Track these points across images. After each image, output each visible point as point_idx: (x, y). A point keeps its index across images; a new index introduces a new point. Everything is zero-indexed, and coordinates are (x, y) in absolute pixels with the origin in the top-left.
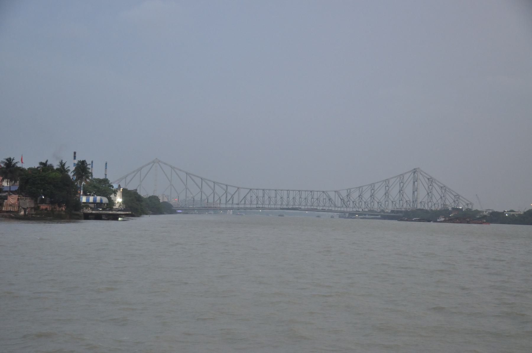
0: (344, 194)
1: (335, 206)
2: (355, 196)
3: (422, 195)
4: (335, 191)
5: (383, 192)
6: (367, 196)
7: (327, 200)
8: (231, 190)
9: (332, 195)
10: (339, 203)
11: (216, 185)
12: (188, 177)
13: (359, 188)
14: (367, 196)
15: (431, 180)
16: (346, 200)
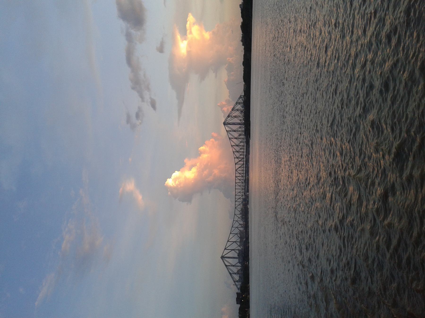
0: (237, 160)
1: (243, 164)
2: (238, 155)
3: (236, 120)
4: (236, 165)
5: (235, 140)
6: (238, 149)
7: (240, 169)
8: (236, 219)
9: (237, 166)
10: (242, 163)
11: (233, 227)
12: (229, 241)
13: (234, 153)
14: (238, 149)
15: (229, 116)
16: (240, 159)
